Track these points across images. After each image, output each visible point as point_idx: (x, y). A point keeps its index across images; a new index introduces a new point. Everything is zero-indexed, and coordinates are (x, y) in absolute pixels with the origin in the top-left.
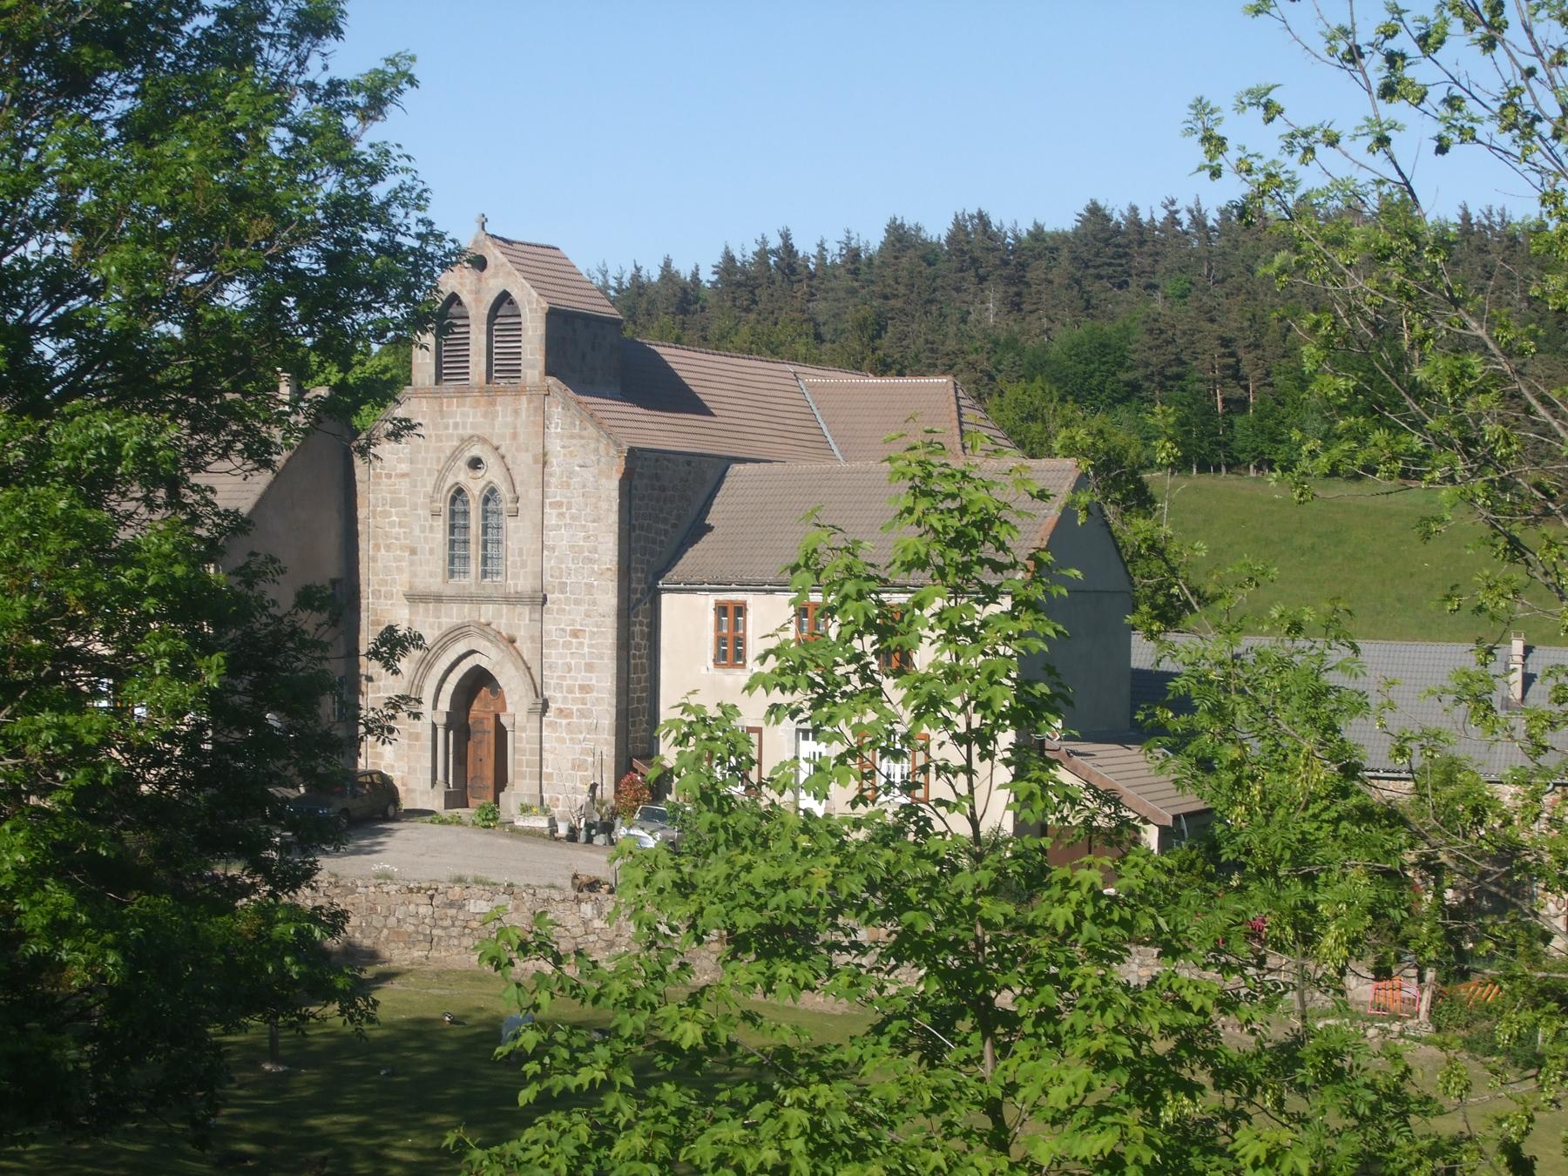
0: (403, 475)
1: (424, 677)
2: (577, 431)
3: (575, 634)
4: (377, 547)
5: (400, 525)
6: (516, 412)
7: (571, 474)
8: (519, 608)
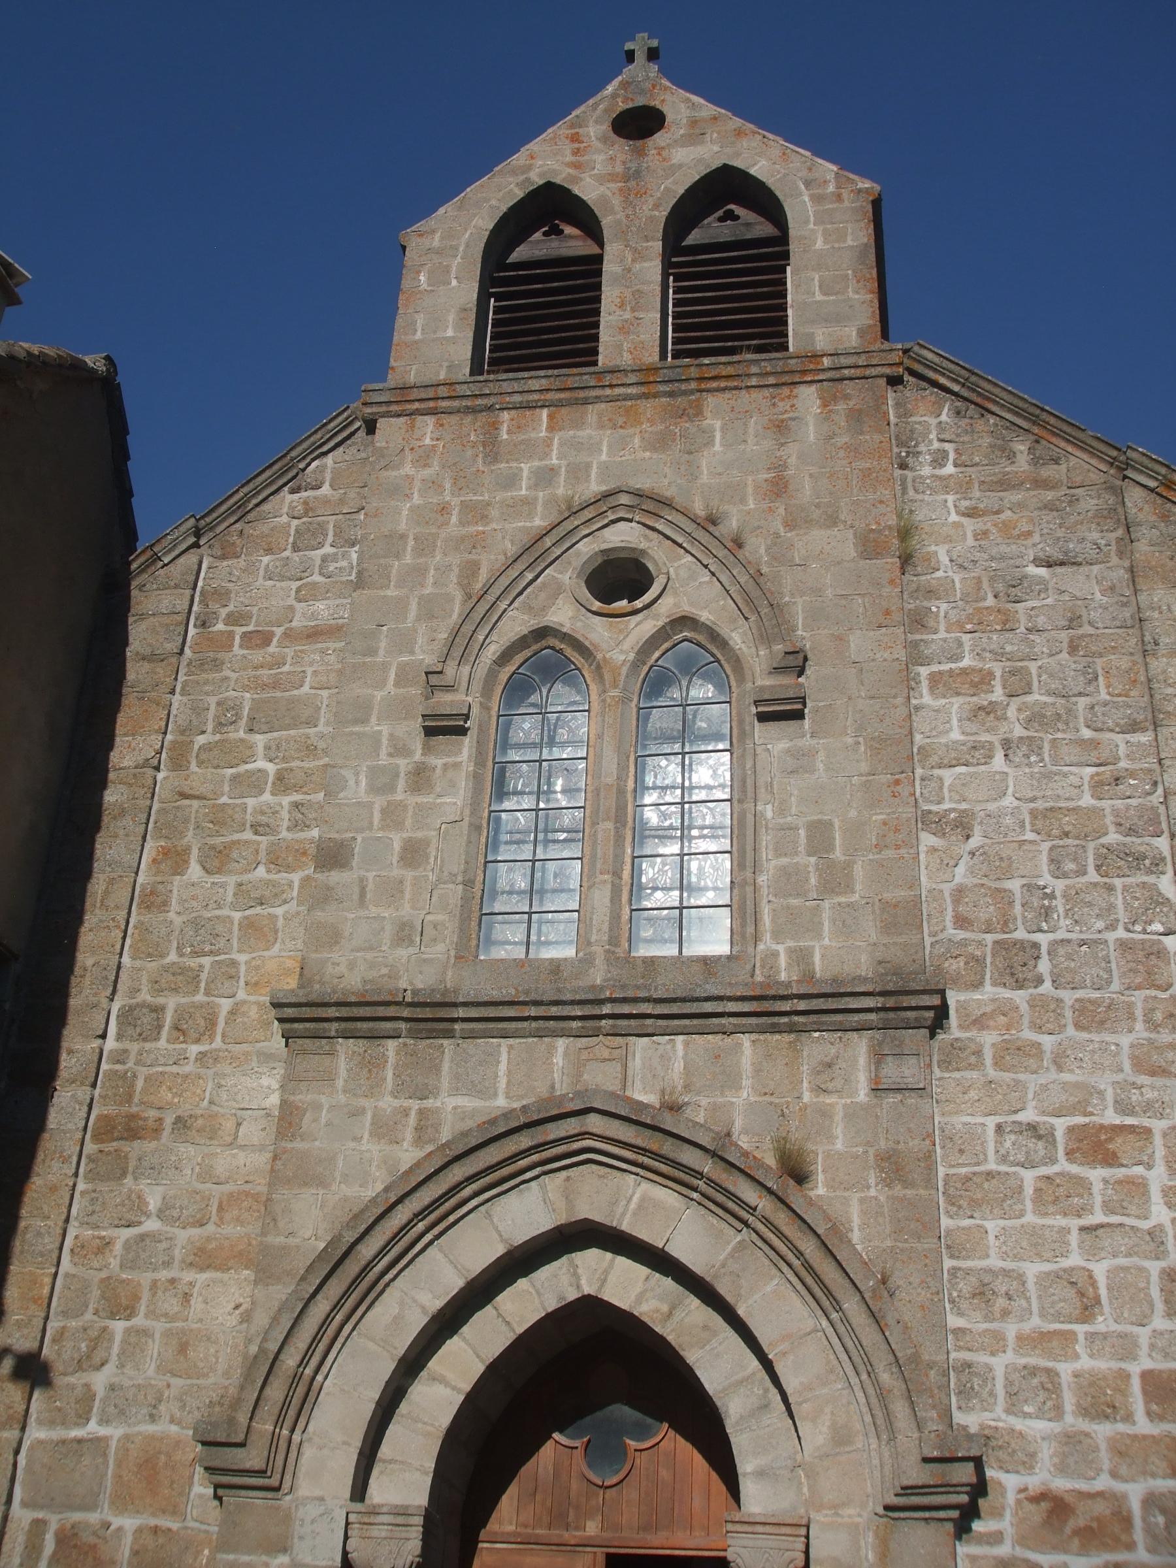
0: (314, 634)
1: (327, 1340)
2: (1023, 463)
3: (1096, 1145)
4: (174, 859)
5: (282, 783)
6: (781, 428)
7: (1015, 588)
8: (818, 1047)
